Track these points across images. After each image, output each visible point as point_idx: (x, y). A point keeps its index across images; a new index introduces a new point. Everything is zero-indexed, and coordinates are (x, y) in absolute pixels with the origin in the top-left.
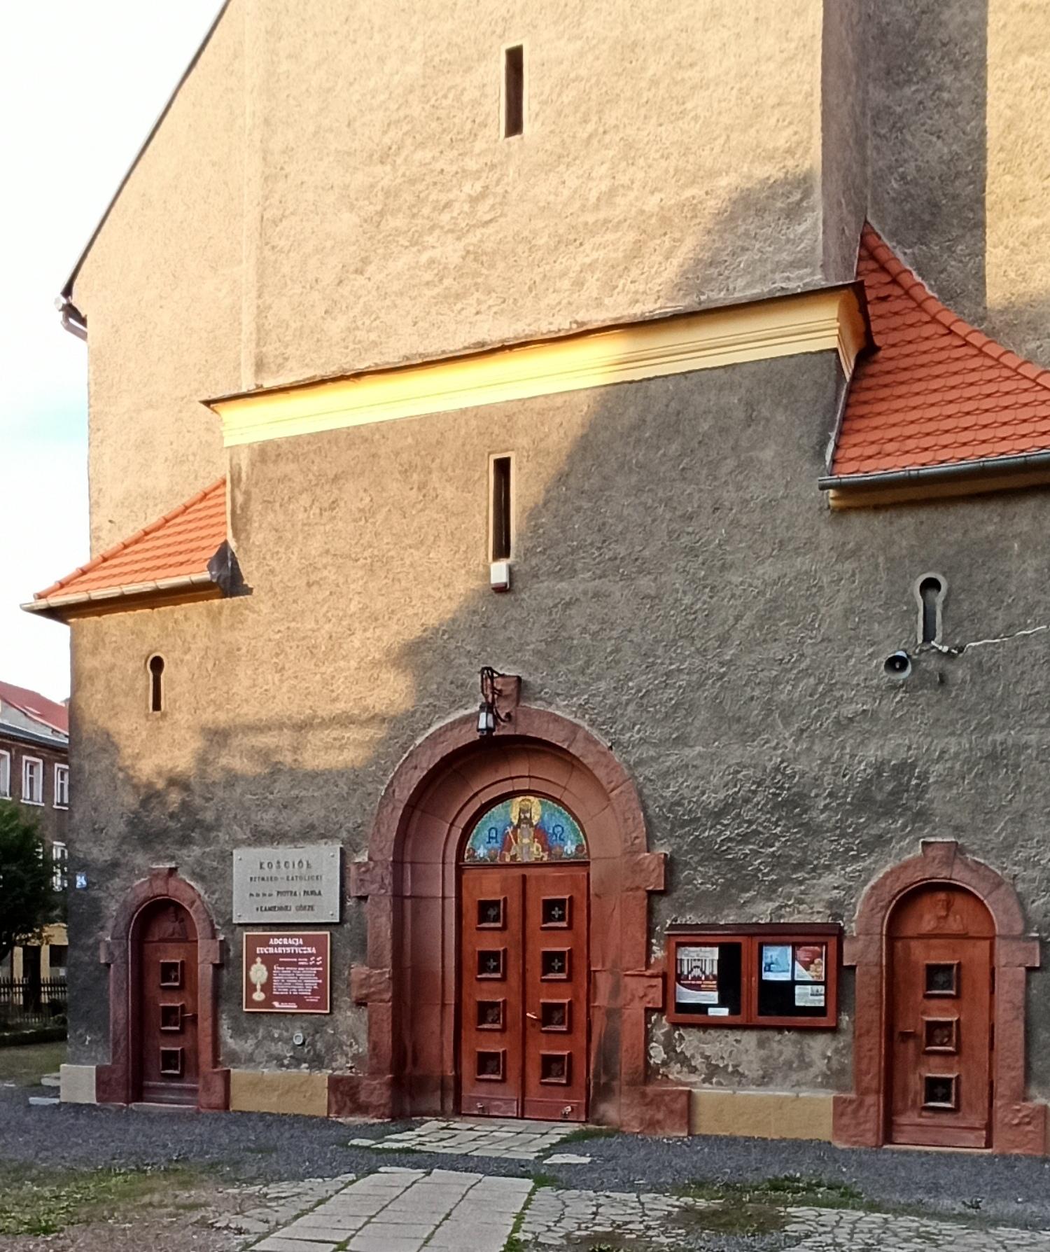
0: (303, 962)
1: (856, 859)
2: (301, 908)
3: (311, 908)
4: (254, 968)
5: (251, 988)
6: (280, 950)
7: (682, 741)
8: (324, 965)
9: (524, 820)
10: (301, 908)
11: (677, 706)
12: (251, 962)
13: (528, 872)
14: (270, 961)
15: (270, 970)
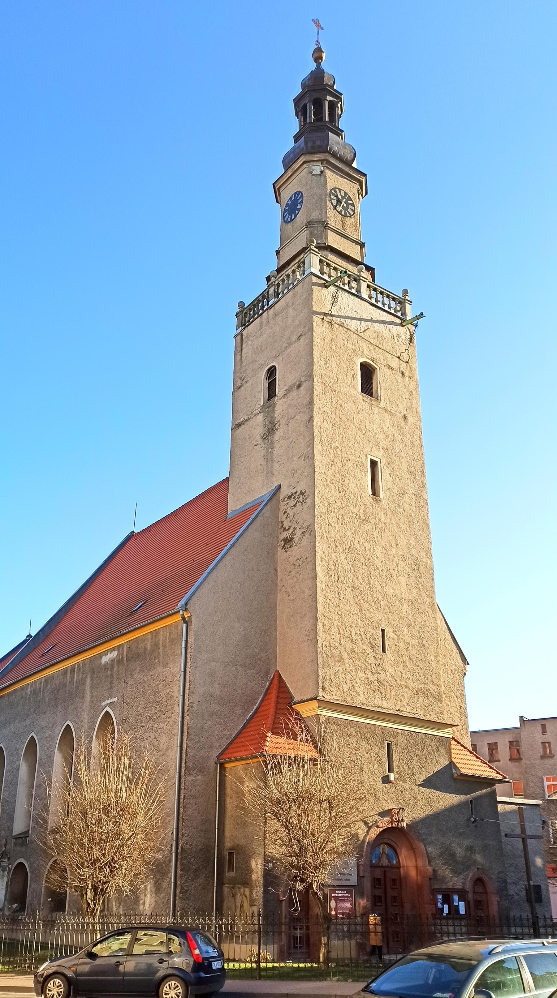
0: (346, 899)
1: (466, 871)
2: (346, 880)
3: (349, 880)
4: (331, 902)
5: (331, 909)
6: (339, 895)
7: (431, 834)
8: (352, 901)
9: (384, 852)
10: (346, 880)
11: (430, 824)
12: (331, 900)
13: (387, 869)
14: (336, 899)
15: (336, 903)
